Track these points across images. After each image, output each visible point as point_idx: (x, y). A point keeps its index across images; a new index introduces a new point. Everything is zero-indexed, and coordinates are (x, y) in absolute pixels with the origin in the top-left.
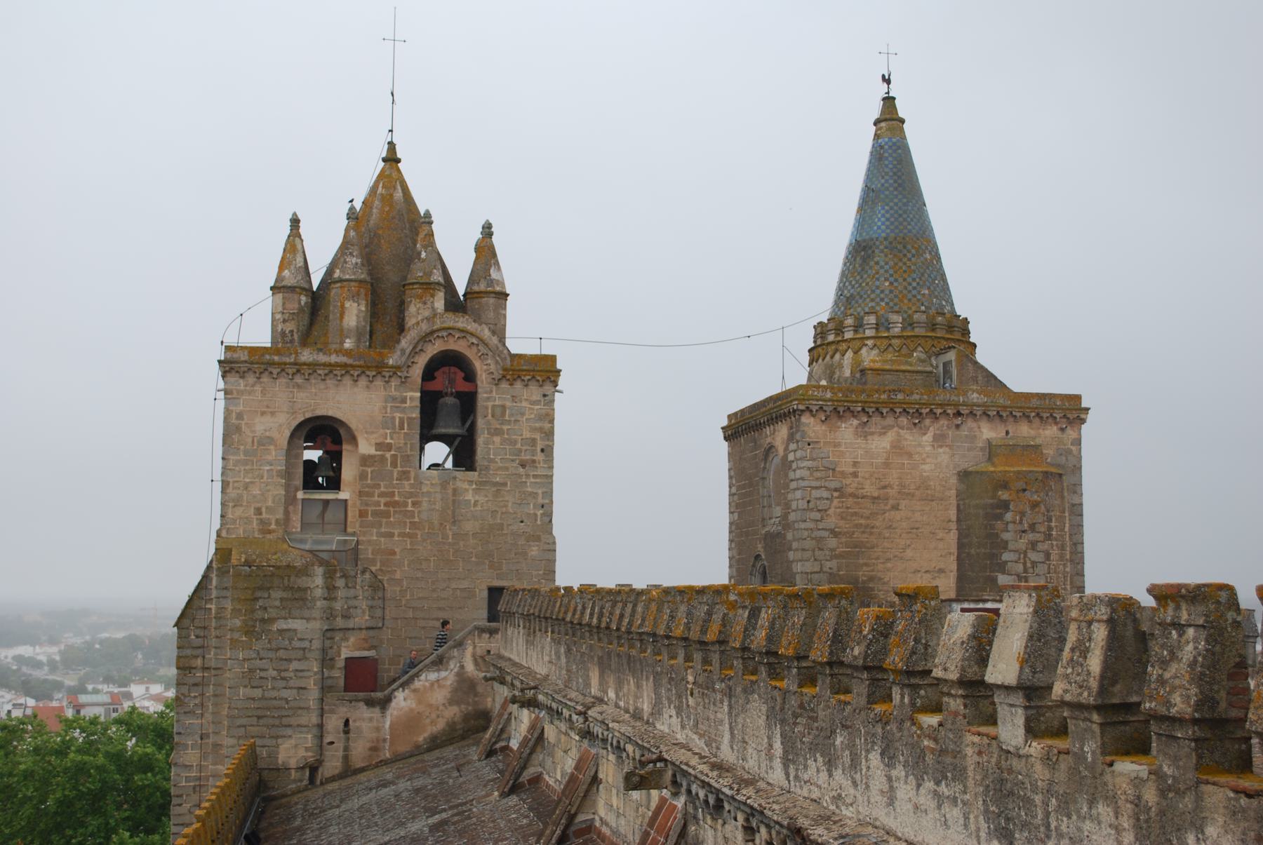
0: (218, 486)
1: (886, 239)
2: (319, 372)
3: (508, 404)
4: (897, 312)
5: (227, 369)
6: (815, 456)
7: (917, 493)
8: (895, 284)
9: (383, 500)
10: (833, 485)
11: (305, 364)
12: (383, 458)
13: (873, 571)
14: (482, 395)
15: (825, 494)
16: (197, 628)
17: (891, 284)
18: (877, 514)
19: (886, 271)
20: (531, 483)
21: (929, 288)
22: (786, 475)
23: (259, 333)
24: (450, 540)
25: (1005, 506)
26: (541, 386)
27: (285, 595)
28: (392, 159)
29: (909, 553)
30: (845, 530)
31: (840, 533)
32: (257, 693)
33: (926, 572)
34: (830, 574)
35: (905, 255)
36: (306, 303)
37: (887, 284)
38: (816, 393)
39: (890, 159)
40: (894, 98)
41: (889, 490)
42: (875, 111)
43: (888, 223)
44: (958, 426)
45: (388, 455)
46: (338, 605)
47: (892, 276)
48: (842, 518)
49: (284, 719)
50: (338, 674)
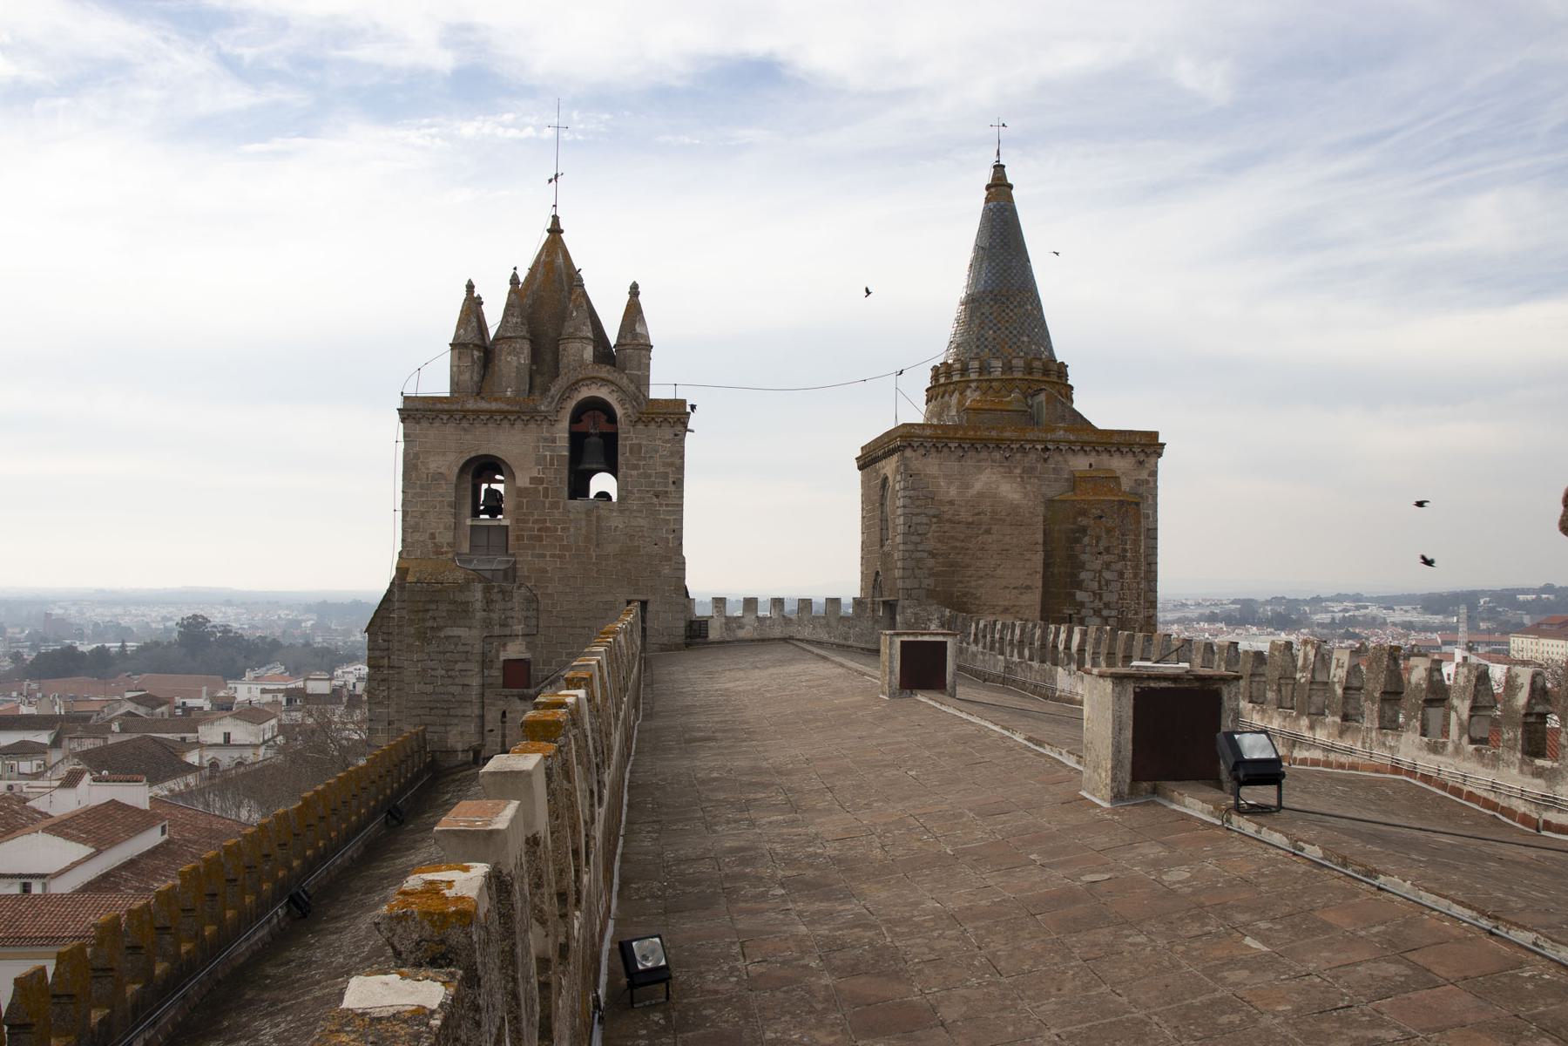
0: (399, 515)
1: (991, 292)
2: (482, 417)
3: (644, 443)
4: (998, 358)
5: (405, 416)
6: (916, 487)
7: (1008, 519)
8: (999, 332)
9: (536, 527)
10: (932, 512)
11: (469, 411)
12: (536, 491)
13: (966, 587)
14: (621, 436)
15: (925, 520)
16: (384, 633)
17: (995, 332)
18: (971, 537)
19: (991, 321)
20: (664, 511)
21: (1028, 336)
23: (437, 383)
24: (594, 560)
25: (1084, 530)
26: (672, 427)
27: (451, 607)
28: (555, 230)
29: (999, 572)
30: (942, 552)
31: (937, 554)
32: (429, 689)
33: (1014, 588)
34: (928, 590)
35: (1008, 307)
36: (478, 358)
37: (991, 332)
38: (918, 431)
39: (998, 220)
40: (1004, 166)
41: (982, 516)
42: (987, 176)
43: (994, 278)
44: (1045, 460)
45: (541, 488)
46: (495, 616)
47: (995, 325)
48: (940, 541)
49: (451, 710)
50: (496, 673)
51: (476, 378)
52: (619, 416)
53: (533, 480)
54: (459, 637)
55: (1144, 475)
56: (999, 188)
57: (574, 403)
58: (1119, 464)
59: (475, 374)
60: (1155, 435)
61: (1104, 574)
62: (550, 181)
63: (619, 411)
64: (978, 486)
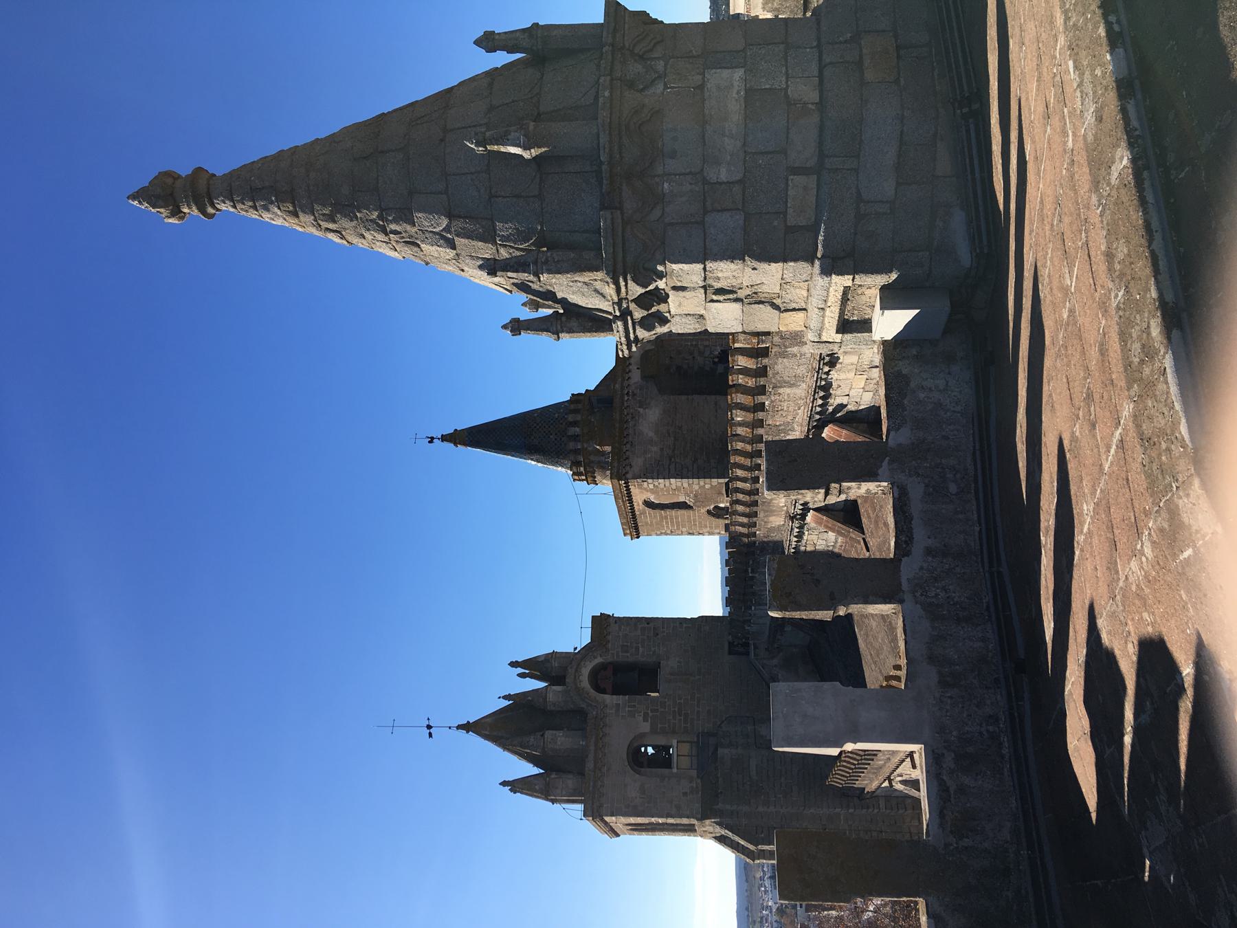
2: (600, 756)
9: (678, 717)
17: (551, 434)
28: (467, 727)
40: (442, 435)
45: (650, 714)
51: (571, 776)
53: (645, 720)
54: (757, 765)
56: (457, 438)
57: (592, 691)
61: (707, 356)
62: (430, 735)
63: (599, 660)
64: (651, 434)
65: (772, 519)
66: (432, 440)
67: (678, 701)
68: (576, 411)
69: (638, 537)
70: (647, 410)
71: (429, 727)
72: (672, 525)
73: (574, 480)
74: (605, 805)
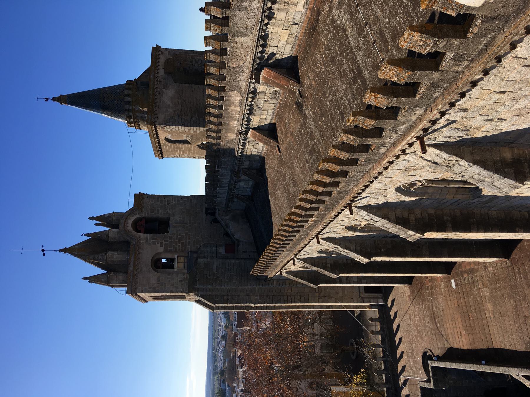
9: (178, 244)
16: (215, 298)
22: (174, 132)
28: (65, 250)
33: (204, 94)
40: (53, 98)
42: (58, 104)
51: (122, 274)
52: (139, 216)
53: (161, 245)
54: (217, 267)
55: (167, 52)
56: (61, 99)
57: (133, 231)
58: (162, 60)
59: (120, 274)
60: (153, 48)
62: (44, 254)
63: (138, 216)
64: (169, 103)
65: (229, 134)
66: (47, 100)
67: (179, 236)
68: (129, 89)
69: (162, 158)
70: (167, 90)
71: (43, 250)
72: (180, 152)
73: (128, 126)
74: (138, 288)
